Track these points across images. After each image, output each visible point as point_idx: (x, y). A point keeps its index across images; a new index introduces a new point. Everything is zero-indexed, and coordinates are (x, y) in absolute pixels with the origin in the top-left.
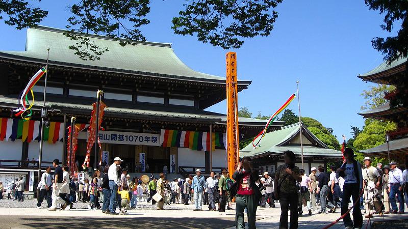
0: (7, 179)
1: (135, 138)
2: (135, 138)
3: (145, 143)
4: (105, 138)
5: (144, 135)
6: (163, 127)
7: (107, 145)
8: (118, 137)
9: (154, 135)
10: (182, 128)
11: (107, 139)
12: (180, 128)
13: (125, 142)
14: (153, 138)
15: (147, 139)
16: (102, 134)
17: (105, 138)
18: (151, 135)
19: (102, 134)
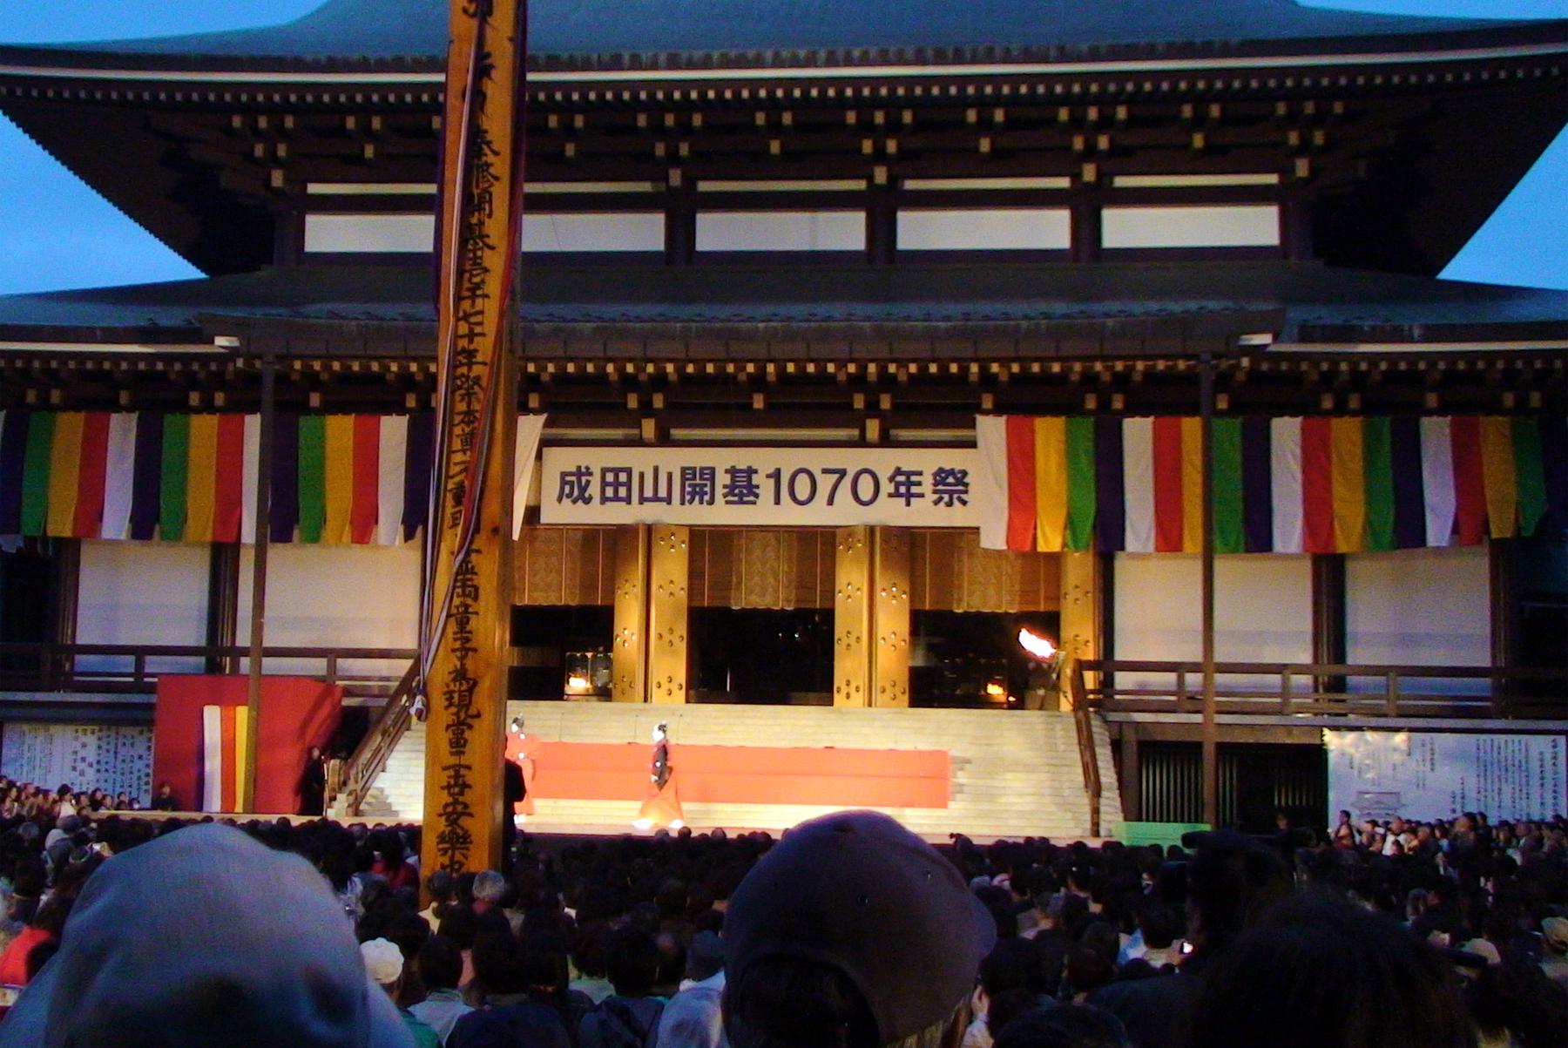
0: (82, 753)
1: (826, 483)
2: (826, 483)
3: (891, 512)
4: (648, 493)
5: (885, 461)
6: (987, 402)
7: (878, 535)
8: (723, 479)
9: (951, 459)
10: (1118, 403)
11: (656, 499)
12: (1104, 406)
13: (764, 512)
14: (941, 476)
15: (905, 487)
16: (629, 471)
17: (648, 493)
18: (926, 462)
19: (629, 471)
